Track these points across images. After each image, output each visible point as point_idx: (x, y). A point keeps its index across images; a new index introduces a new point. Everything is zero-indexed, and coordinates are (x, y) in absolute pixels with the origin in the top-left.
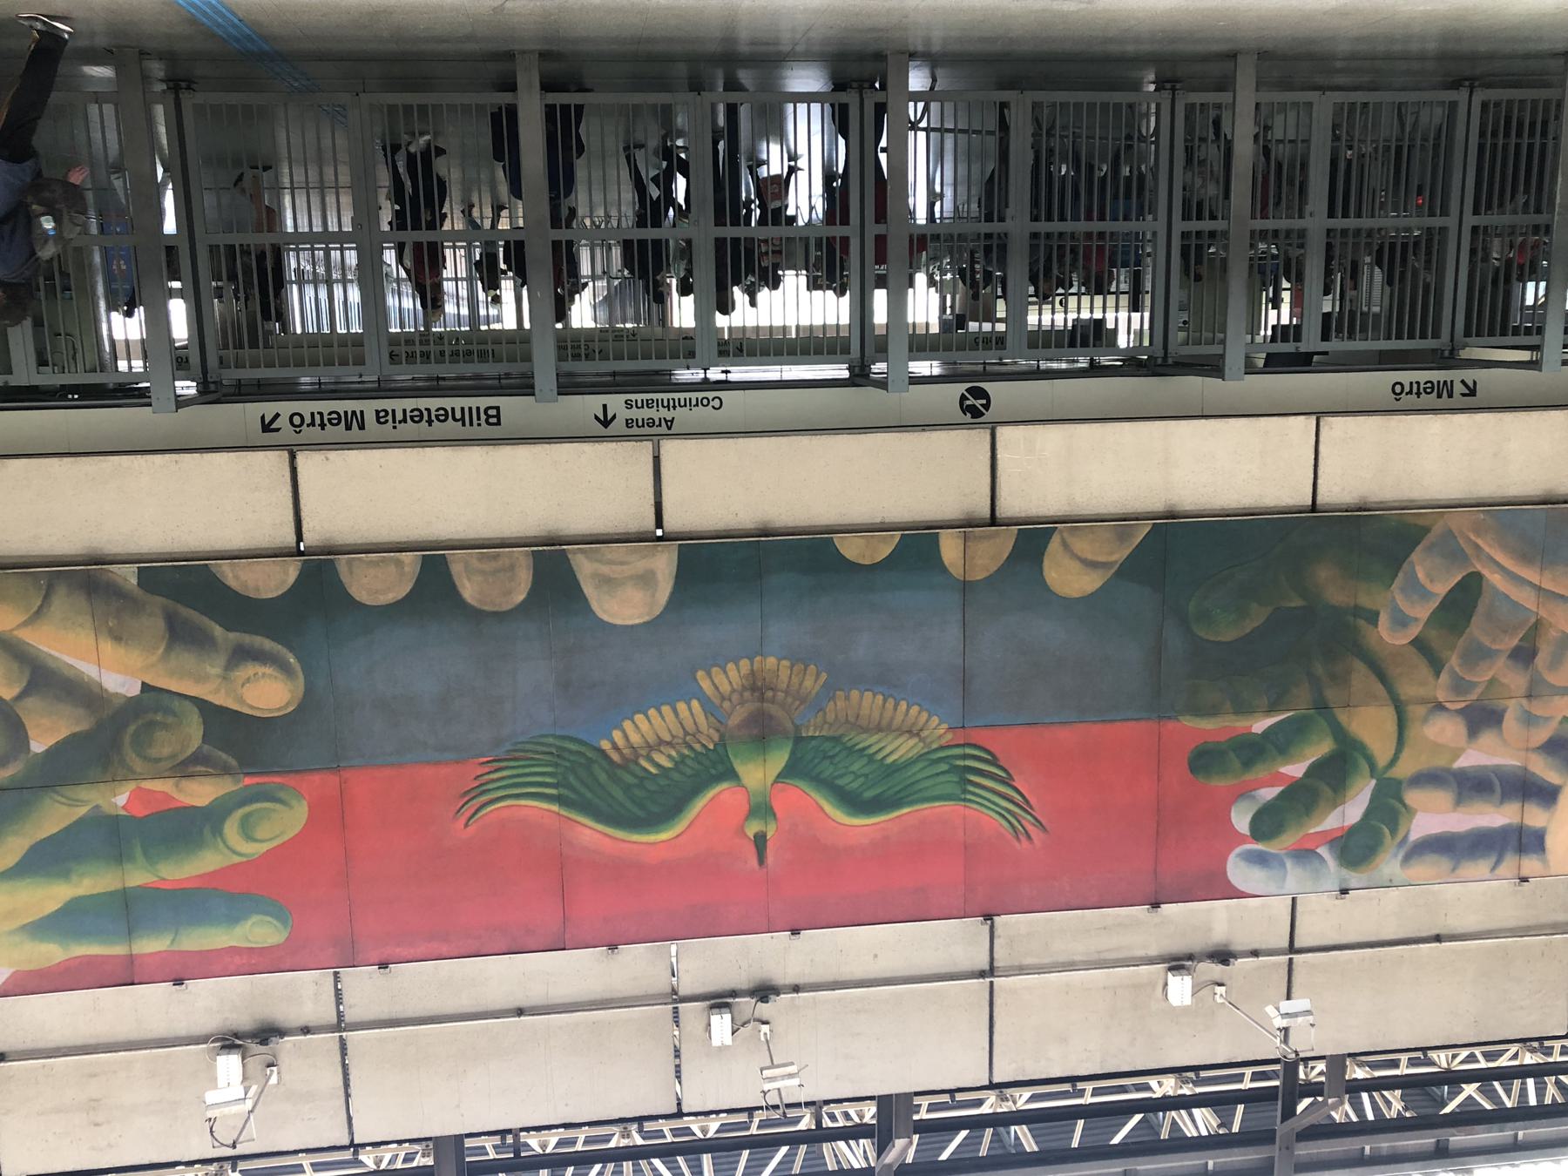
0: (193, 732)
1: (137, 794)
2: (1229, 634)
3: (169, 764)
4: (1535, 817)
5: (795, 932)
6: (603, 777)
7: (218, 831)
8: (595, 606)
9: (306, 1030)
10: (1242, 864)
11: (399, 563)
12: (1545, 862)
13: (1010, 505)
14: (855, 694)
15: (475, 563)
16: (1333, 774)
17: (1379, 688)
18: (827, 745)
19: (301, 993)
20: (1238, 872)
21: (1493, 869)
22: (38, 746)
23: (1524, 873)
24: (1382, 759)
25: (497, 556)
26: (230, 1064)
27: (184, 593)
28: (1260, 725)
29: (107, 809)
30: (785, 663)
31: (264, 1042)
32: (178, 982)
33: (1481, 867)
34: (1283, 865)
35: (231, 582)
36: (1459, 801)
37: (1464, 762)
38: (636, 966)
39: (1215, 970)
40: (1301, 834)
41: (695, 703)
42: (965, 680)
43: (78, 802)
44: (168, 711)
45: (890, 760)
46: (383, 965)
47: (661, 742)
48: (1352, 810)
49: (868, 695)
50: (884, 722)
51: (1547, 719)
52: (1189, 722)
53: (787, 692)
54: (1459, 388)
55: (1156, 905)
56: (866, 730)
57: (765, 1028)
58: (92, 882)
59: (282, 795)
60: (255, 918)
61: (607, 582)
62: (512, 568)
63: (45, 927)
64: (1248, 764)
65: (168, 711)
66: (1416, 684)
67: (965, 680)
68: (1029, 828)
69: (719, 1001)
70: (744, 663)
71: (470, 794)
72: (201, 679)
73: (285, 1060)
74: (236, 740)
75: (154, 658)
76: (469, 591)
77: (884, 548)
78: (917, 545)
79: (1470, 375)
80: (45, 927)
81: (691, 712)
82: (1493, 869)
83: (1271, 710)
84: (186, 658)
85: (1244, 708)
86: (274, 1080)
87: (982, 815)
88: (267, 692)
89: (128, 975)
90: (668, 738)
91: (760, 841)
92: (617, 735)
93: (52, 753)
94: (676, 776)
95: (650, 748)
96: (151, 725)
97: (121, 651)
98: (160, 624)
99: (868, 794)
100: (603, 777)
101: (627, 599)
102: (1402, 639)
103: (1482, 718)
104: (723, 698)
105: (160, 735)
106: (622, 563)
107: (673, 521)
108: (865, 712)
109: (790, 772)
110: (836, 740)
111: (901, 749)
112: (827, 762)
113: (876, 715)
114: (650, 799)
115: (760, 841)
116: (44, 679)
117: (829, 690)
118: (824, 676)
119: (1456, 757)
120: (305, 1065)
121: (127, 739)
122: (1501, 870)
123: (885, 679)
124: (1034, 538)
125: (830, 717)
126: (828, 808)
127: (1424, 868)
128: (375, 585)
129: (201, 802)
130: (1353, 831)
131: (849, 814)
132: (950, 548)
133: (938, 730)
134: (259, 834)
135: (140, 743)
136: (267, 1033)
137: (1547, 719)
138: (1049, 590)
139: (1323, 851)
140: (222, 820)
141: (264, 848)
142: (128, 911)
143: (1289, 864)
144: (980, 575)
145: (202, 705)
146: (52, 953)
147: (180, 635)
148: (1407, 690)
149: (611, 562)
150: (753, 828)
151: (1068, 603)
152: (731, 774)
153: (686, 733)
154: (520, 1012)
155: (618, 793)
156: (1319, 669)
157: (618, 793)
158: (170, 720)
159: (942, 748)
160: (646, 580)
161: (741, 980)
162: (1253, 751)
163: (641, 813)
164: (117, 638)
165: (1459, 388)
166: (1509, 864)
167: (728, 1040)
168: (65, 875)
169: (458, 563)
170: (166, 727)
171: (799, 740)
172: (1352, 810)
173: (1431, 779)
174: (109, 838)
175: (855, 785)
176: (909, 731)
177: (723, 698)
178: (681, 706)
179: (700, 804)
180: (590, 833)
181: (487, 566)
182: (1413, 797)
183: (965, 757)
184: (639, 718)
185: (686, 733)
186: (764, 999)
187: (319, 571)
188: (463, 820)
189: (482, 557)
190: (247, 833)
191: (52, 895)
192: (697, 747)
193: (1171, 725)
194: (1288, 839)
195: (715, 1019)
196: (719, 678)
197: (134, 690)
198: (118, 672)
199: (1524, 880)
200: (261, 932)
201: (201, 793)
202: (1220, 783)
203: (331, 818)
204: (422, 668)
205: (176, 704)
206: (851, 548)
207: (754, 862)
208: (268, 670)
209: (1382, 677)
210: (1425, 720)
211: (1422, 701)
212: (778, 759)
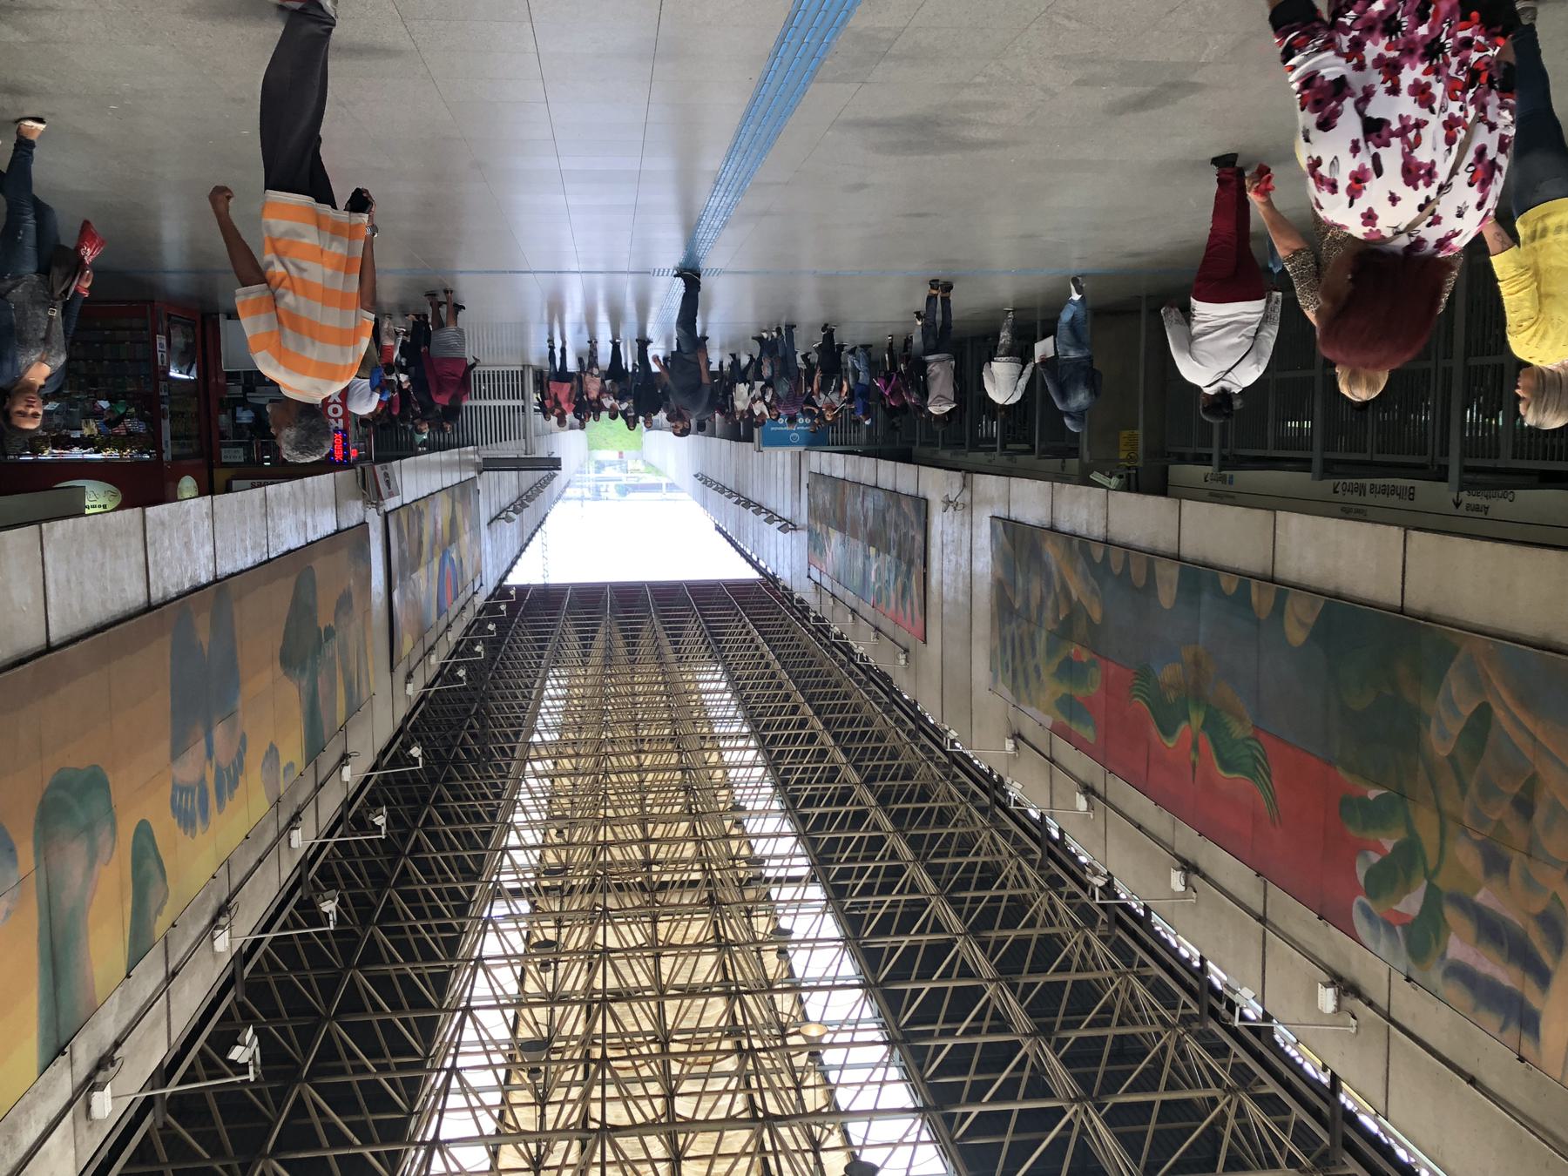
23: (1524, 1053)
24: (1431, 867)
28: (1373, 793)
33: (1492, 1021)
37: (1480, 897)
83: (1378, 784)
119: (1477, 891)
122: (1506, 1035)
139: (1399, 929)
148: (1447, 805)
152: (1187, 718)
154: (1139, 827)
172: (1411, 904)
180: (1154, 730)
182: (1451, 913)
202: (1353, 832)
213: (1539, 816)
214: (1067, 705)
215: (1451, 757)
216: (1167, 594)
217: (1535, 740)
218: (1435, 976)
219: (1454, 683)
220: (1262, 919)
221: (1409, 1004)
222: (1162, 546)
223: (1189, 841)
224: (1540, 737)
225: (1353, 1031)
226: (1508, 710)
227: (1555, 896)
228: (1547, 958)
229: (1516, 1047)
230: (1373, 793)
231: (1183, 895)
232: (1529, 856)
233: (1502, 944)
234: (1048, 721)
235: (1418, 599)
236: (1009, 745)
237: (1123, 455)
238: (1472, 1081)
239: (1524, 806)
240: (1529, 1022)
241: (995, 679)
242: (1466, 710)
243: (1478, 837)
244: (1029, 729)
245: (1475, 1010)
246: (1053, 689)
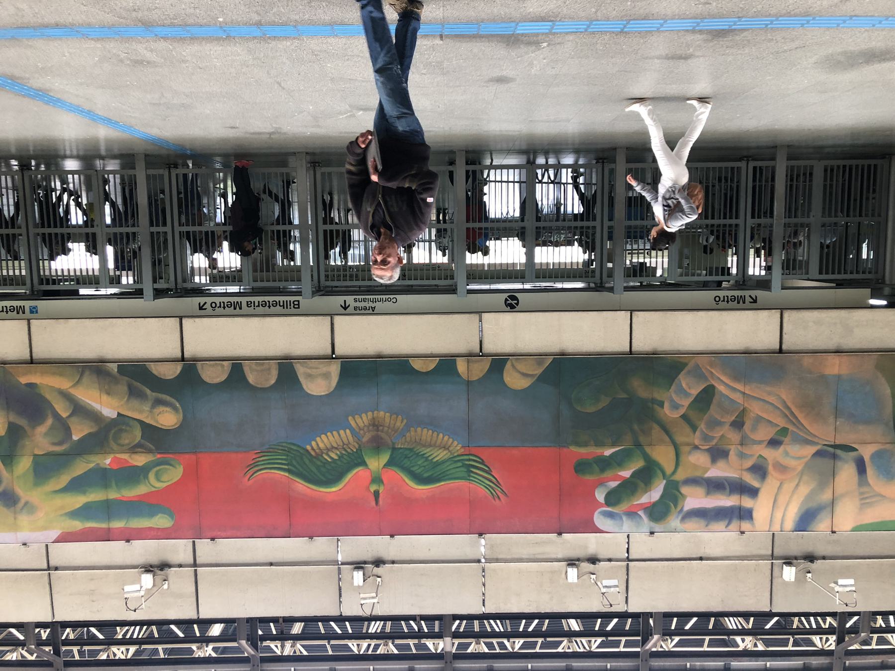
0: (138, 434)
1: (115, 460)
2: (591, 409)
3: (127, 447)
4: (747, 502)
5: (392, 536)
6: (307, 462)
7: (146, 477)
8: (305, 387)
9: (180, 566)
10: (602, 517)
11: (223, 366)
12: (753, 524)
13: (489, 348)
14: (419, 429)
15: (254, 367)
16: (646, 476)
17: (667, 439)
18: (407, 452)
19: (178, 549)
20: (599, 520)
21: (727, 527)
22: (75, 438)
23: (742, 529)
25: (263, 364)
26: (147, 580)
27: (135, 375)
28: (608, 452)
29: (102, 466)
30: (388, 414)
31: (162, 570)
32: (128, 541)
33: (721, 525)
34: (621, 518)
35: (155, 372)
36: (708, 493)
37: (709, 474)
38: (321, 546)
39: (586, 566)
40: (630, 504)
41: (348, 431)
42: (469, 425)
43: (89, 462)
44: (128, 425)
45: (435, 460)
46: (213, 539)
47: (333, 447)
48: (655, 494)
49: (425, 430)
50: (433, 442)
51: (751, 456)
52: (573, 449)
53: (389, 427)
54: (748, 299)
55: (560, 534)
56: (424, 446)
57: (379, 579)
58: (95, 496)
59: (172, 463)
60: (160, 515)
61: (309, 376)
62: (269, 369)
63: (75, 514)
64: (602, 470)
65: (128, 425)
66: (683, 435)
67: (469, 425)
68: (500, 494)
69: (359, 565)
70: (370, 413)
71: (251, 466)
72: (141, 412)
73: (171, 579)
74: (155, 438)
75: (122, 403)
76: (251, 379)
77: (432, 365)
78: (446, 364)
79: (754, 293)
80: (75, 514)
81: (346, 435)
82: (727, 527)
83: (613, 445)
84: (135, 403)
85: (600, 444)
86: (166, 587)
87: (478, 487)
88: (167, 418)
89: (107, 536)
90: (335, 445)
91: (376, 494)
92: (313, 443)
93: (81, 440)
94: (339, 463)
95: (328, 450)
96: (121, 430)
97: (110, 399)
98: (126, 388)
99: (426, 475)
100: (307, 462)
101: (319, 384)
102: (676, 415)
103: (718, 454)
104: (360, 429)
105: (124, 435)
106: (317, 368)
107: (339, 351)
108: (424, 438)
109: (389, 464)
110: (411, 450)
111: (440, 455)
112: (406, 460)
113: (429, 440)
114: (329, 473)
115: (376, 494)
116: (79, 410)
117: (408, 427)
118: (405, 421)
120: (180, 580)
121: (111, 436)
122: (731, 527)
123: (432, 423)
124: (499, 362)
125: (408, 439)
126: (407, 480)
127: (692, 524)
128: (213, 375)
129: (140, 464)
130: (655, 504)
131: (417, 484)
132: (461, 366)
133: (457, 447)
134: (162, 479)
135: (116, 438)
136: (164, 566)
137: (751, 456)
138: (506, 385)
139: (641, 513)
140: (148, 472)
141: (164, 485)
142: (108, 509)
143: (624, 518)
144: (474, 378)
145: (141, 422)
146: (77, 525)
147: (134, 393)
148: (680, 439)
149: (311, 368)
150: (373, 488)
151: (516, 392)
152: (363, 463)
153: (344, 444)
154: (271, 564)
155: (314, 469)
156: (636, 427)
157: (314, 469)
158: (128, 428)
159: (458, 456)
160: (327, 376)
161: (368, 556)
162: (605, 464)
163: (324, 479)
164: (108, 394)
165: (748, 299)
166: (735, 524)
167: (361, 583)
168: (84, 493)
169: (247, 366)
170: (126, 431)
171: (394, 449)
172: (655, 494)
173: (693, 481)
174: (101, 477)
175: (419, 471)
176: (443, 447)
177: (360, 429)
178: (342, 432)
179: (350, 476)
180: (301, 486)
181: (259, 368)
182: (685, 490)
183: (470, 460)
184: (323, 436)
185: (344, 444)
186: (377, 566)
187: (190, 367)
188: (246, 479)
189: (257, 364)
190: (158, 479)
191: (78, 500)
192: (349, 450)
193: (565, 450)
194: (624, 506)
195: (355, 573)
196: (359, 420)
197: (115, 416)
198: (107, 407)
199: (743, 533)
200: (162, 521)
201: (140, 460)
202: (589, 477)
203: (192, 474)
204: (231, 411)
205: (131, 423)
206: (417, 365)
207: (373, 503)
208: (168, 409)
209: (667, 432)
210: (690, 453)
211: (688, 444)
212: (385, 458)
213: (746, 427)
215: (684, 417)
217: (744, 393)
219: (683, 380)
228: (755, 484)
232: (742, 444)
239: (738, 424)
240: (745, 514)
242: (695, 392)
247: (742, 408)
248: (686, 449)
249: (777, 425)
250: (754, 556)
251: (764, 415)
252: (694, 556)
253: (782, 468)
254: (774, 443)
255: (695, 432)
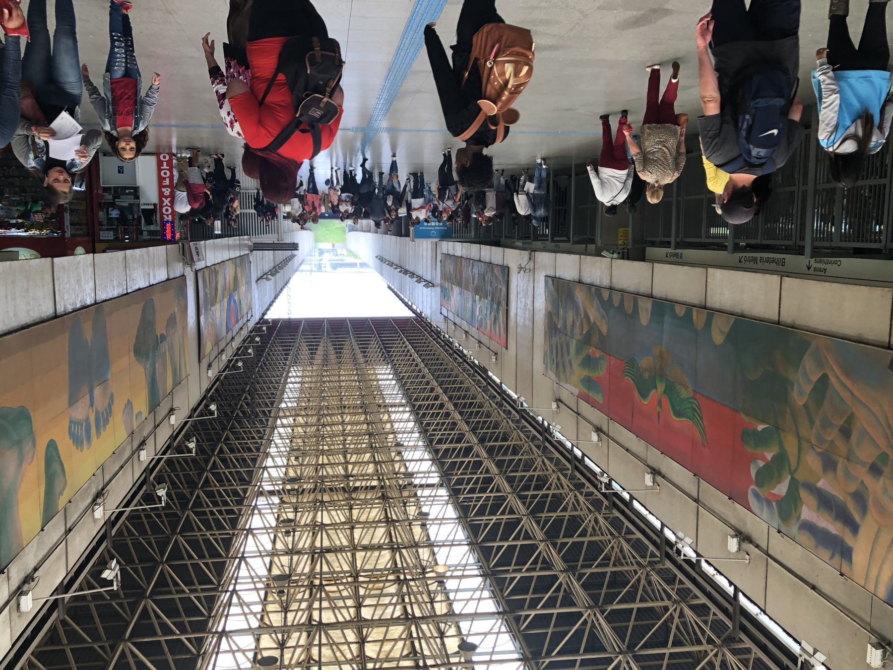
23: (843, 571)
24: (793, 468)
28: (760, 427)
33: (826, 553)
37: (821, 484)
83: (763, 422)
119: (818, 481)
127: (805, 538)
139: (774, 504)
148: (803, 432)
152: (655, 387)
154: (627, 450)
172: (781, 489)
180: (637, 395)
182: (803, 494)
202: (749, 450)
213: (854, 438)
214: (588, 382)
216: (645, 317)
217: (852, 393)
218: (794, 529)
219: (808, 362)
220: (696, 501)
221: (779, 546)
222: (642, 290)
223: (655, 457)
224: (855, 392)
225: (747, 562)
226: (837, 377)
227: (862, 482)
228: (857, 517)
229: (838, 567)
230: (760, 427)
231: (652, 488)
232: (848, 460)
233: (832, 510)
234: (576, 391)
235: (786, 317)
236: (554, 405)
237: (620, 242)
238: (814, 588)
239: (846, 432)
240: (846, 553)
241: (546, 368)
242: (815, 378)
243: (819, 450)
244: (565, 396)
245: (816, 547)
246: (578, 372)
247: (850, 413)
248: (805, 444)
249: (880, 448)
250: (855, 615)
251: (869, 429)
252: (810, 581)
253: (882, 511)
254: (875, 470)
255: (812, 428)
